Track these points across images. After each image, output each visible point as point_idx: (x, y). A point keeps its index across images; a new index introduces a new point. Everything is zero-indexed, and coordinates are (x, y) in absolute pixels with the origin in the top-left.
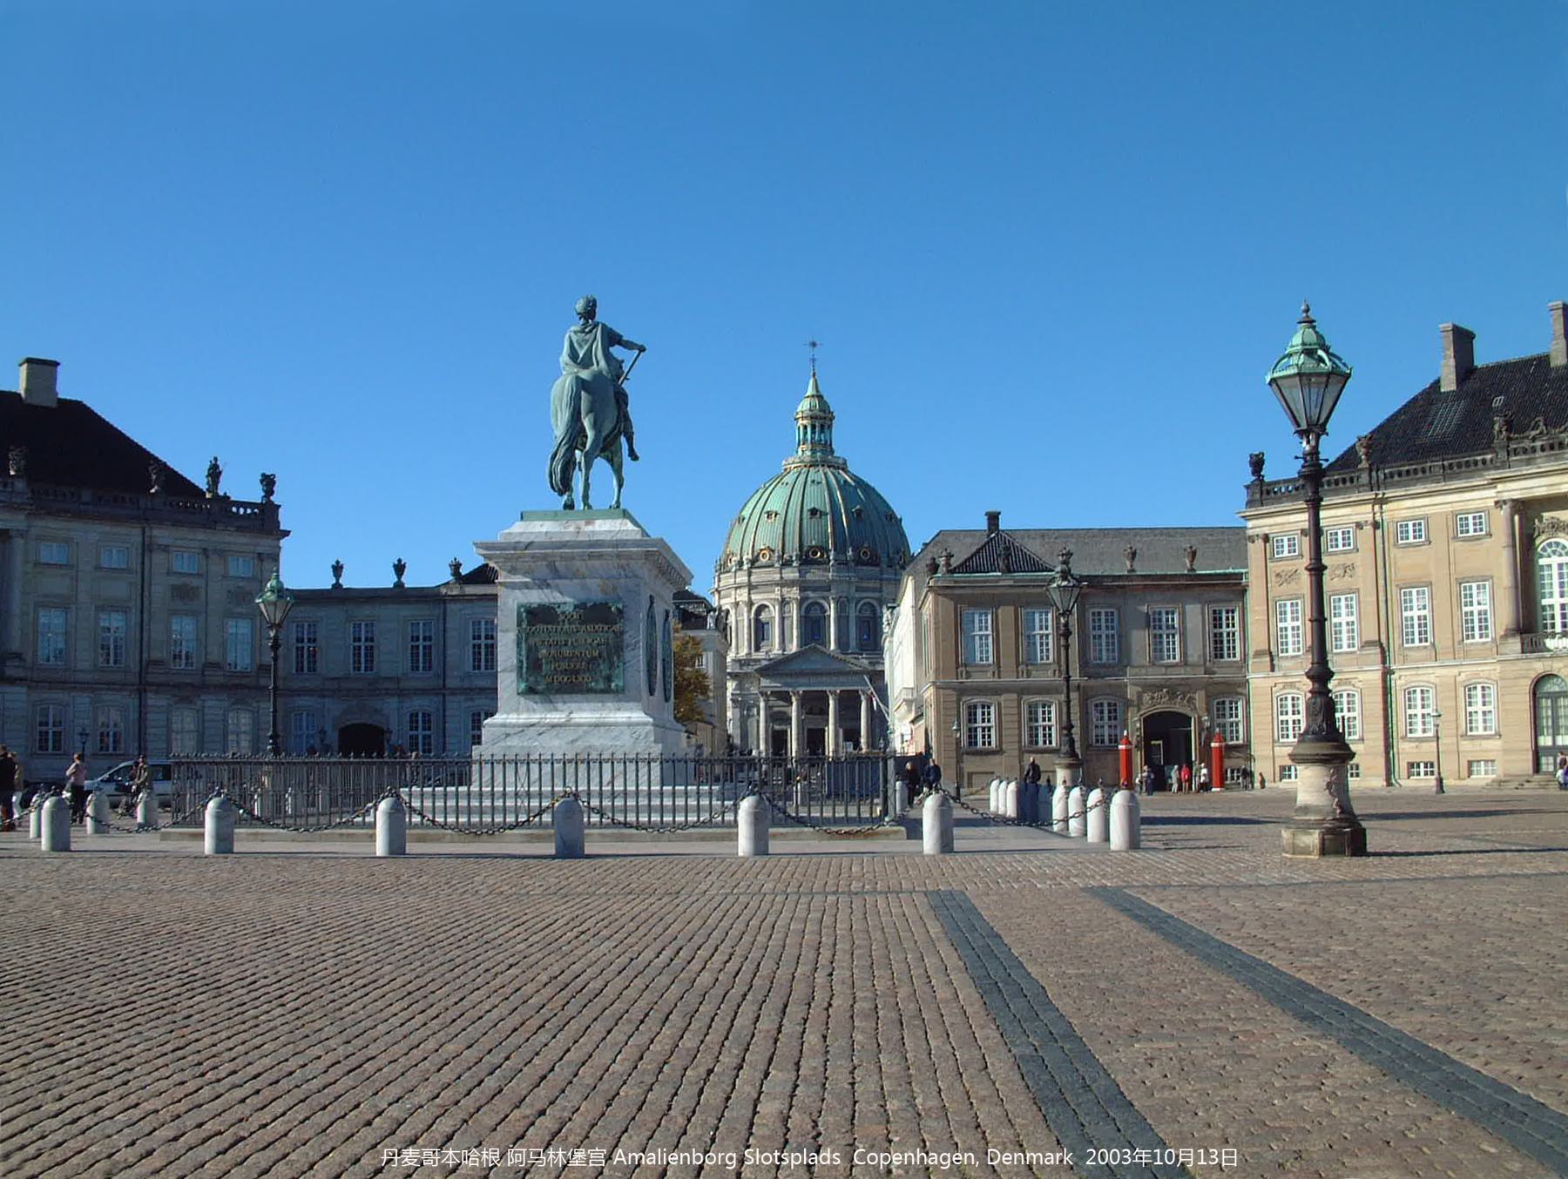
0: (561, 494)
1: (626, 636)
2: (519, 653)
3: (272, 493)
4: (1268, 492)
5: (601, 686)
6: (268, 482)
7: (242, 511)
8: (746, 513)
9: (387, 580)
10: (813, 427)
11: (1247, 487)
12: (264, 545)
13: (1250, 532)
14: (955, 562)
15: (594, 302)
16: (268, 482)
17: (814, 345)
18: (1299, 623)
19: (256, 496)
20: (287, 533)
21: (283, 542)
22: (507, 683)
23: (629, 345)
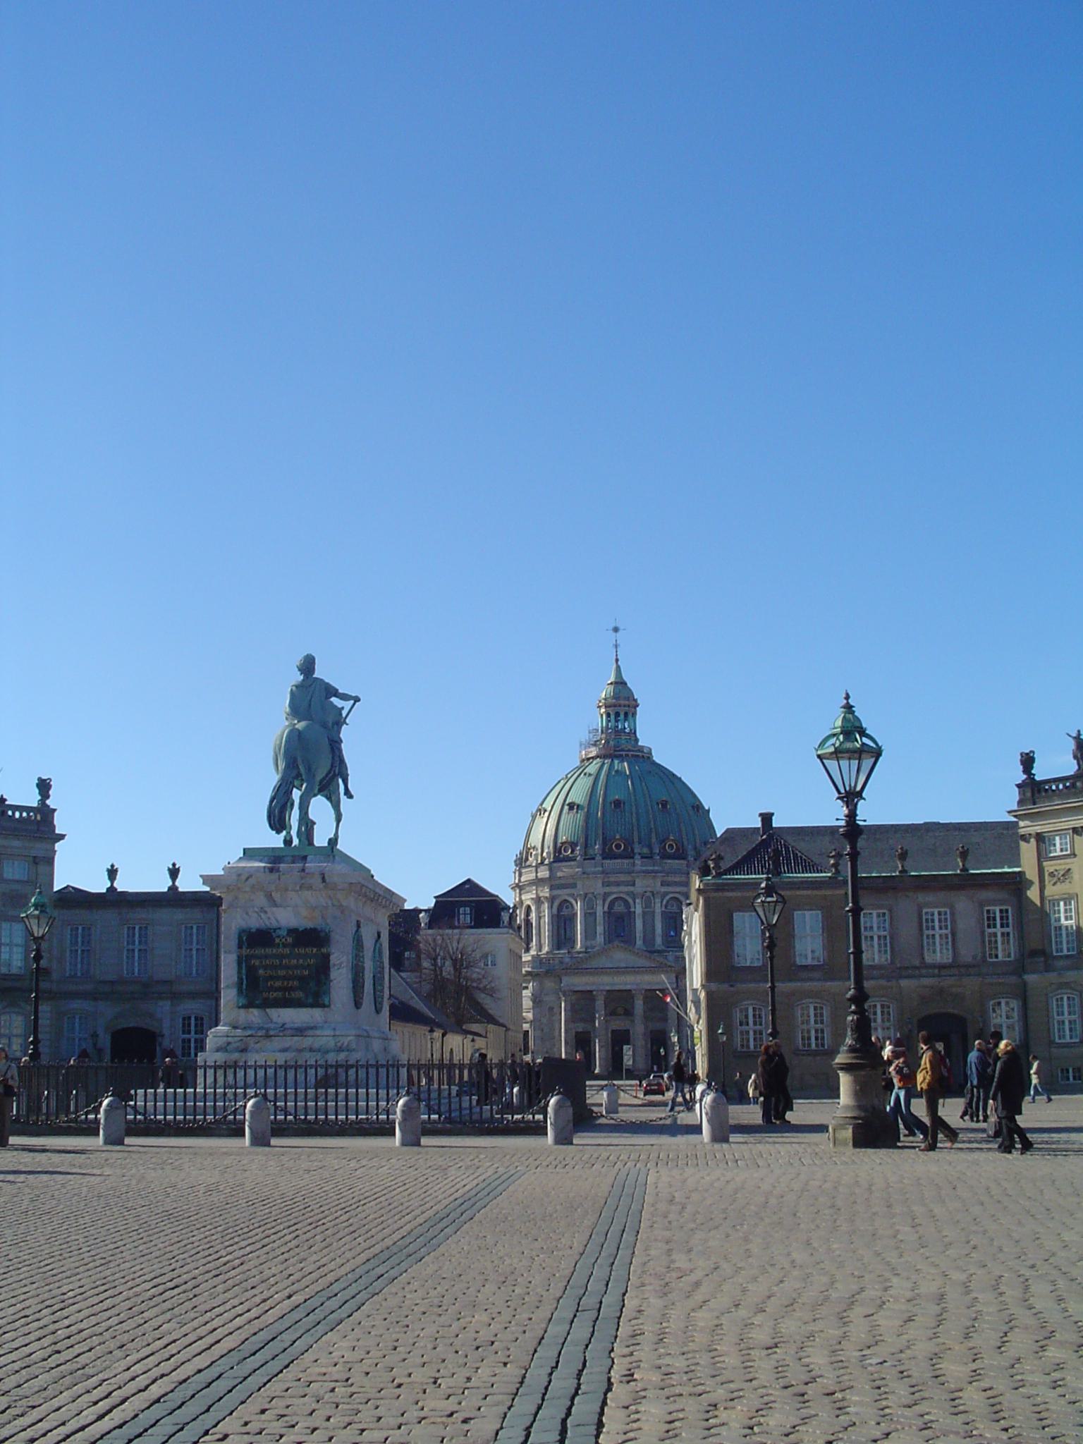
0: (279, 832)
1: (332, 957)
2: (239, 972)
3: (48, 797)
4: (1039, 791)
5: (310, 1000)
6: (44, 786)
7: (17, 815)
8: (547, 805)
9: (161, 885)
10: (617, 714)
11: (1018, 786)
12: (38, 849)
13: (1022, 831)
14: (725, 865)
15: (313, 659)
16: (44, 786)
17: (616, 630)
18: (1010, 930)
19: (33, 799)
20: (62, 837)
21: (57, 846)
22: (228, 996)
23: (345, 697)
